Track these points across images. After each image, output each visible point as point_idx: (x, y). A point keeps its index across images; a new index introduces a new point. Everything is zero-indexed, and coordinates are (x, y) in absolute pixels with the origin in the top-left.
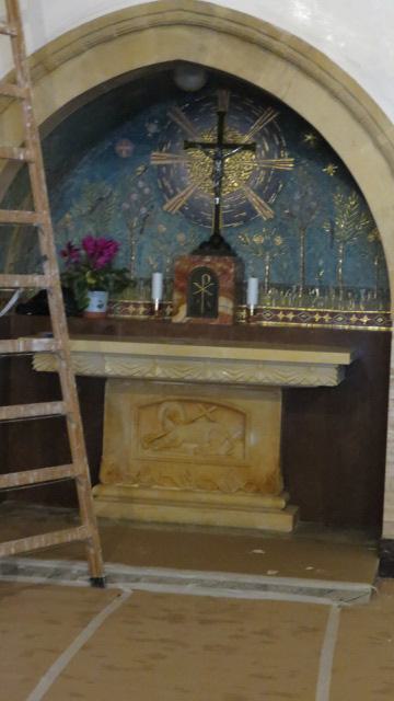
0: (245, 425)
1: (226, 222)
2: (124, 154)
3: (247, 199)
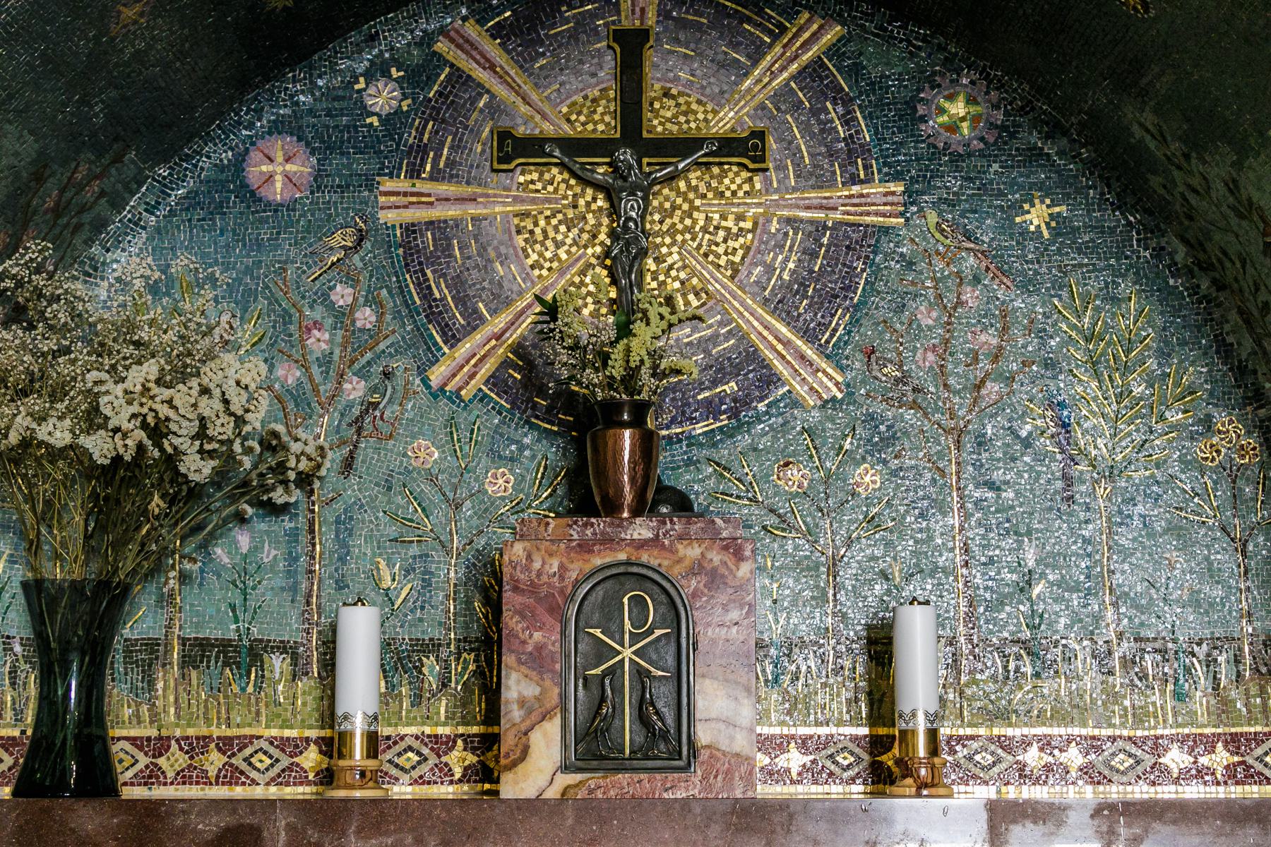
2: (278, 191)
3: (735, 333)
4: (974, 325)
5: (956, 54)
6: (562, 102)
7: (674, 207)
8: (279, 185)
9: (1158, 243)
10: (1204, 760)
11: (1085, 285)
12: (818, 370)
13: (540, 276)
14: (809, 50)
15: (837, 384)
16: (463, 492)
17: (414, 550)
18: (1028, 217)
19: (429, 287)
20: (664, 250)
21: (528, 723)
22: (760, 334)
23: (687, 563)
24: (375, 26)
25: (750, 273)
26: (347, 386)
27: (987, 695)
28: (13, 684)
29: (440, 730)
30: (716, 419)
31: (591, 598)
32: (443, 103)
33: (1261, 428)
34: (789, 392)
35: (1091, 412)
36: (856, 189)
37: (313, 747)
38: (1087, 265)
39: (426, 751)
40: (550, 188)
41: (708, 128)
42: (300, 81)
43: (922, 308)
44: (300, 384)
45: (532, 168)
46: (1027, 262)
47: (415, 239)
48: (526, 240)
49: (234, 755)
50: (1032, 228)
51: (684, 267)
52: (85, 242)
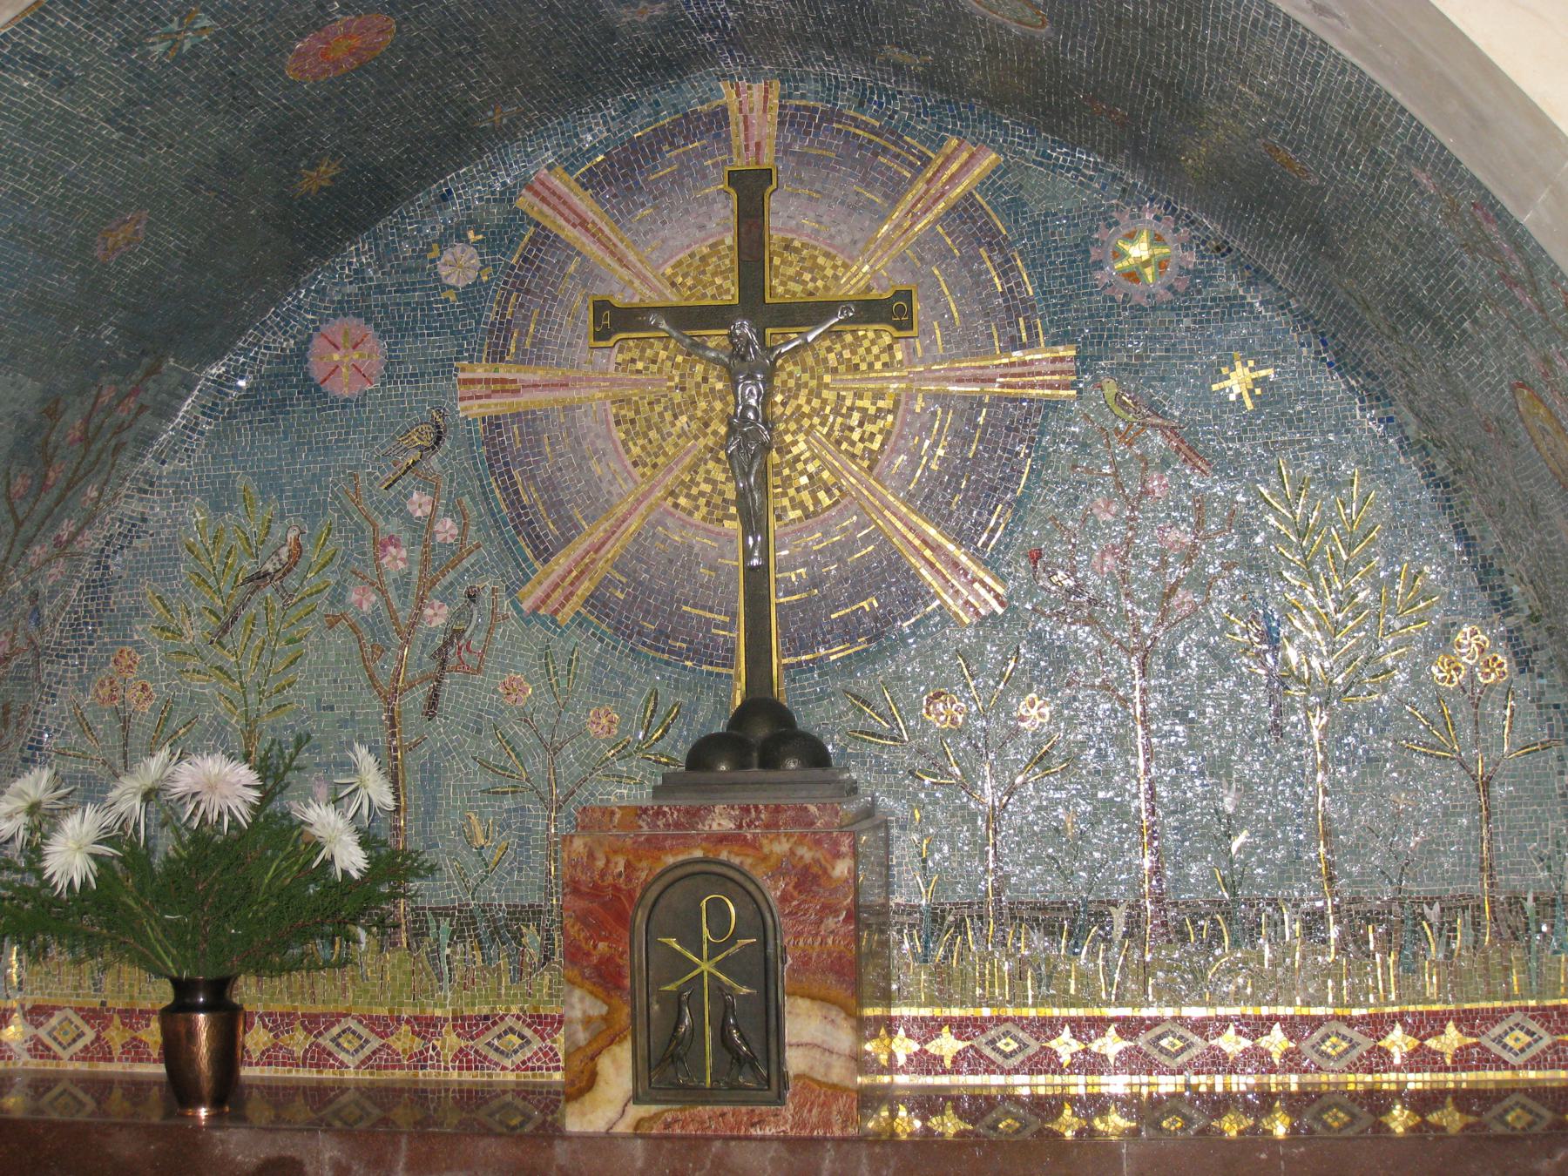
1: (796, 644)
2: (343, 386)
4: (1160, 520)
5: (1135, 185)
6: (665, 262)
7: (799, 387)
9: (1386, 413)
11: (1299, 466)
12: (973, 581)
13: (643, 475)
14: (956, 185)
15: (997, 596)
17: (508, 803)
18: (1227, 383)
19: (517, 492)
21: (595, 1046)
22: (905, 537)
23: (773, 860)
24: (446, 184)
25: (891, 463)
26: (428, 612)
30: (853, 642)
31: (662, 902)
32: (528, 270)
33: (1510, 639)
34: (940, 607)
35: (1306, 624)
37: (405, 1028)
38: (1299, 442)
39: (528, 1033)
40: (654, 368)
41: (839, 287)
42: (365, 253)
43: (1100, 501)
44: (376, 612)
45: (631, 343)
46: (1227, 440)
47: (500, 435)
48: (627, 432)
49: (320, 1034)
50: (1232, 397)
51: (813, 458)
52: (133, 459)
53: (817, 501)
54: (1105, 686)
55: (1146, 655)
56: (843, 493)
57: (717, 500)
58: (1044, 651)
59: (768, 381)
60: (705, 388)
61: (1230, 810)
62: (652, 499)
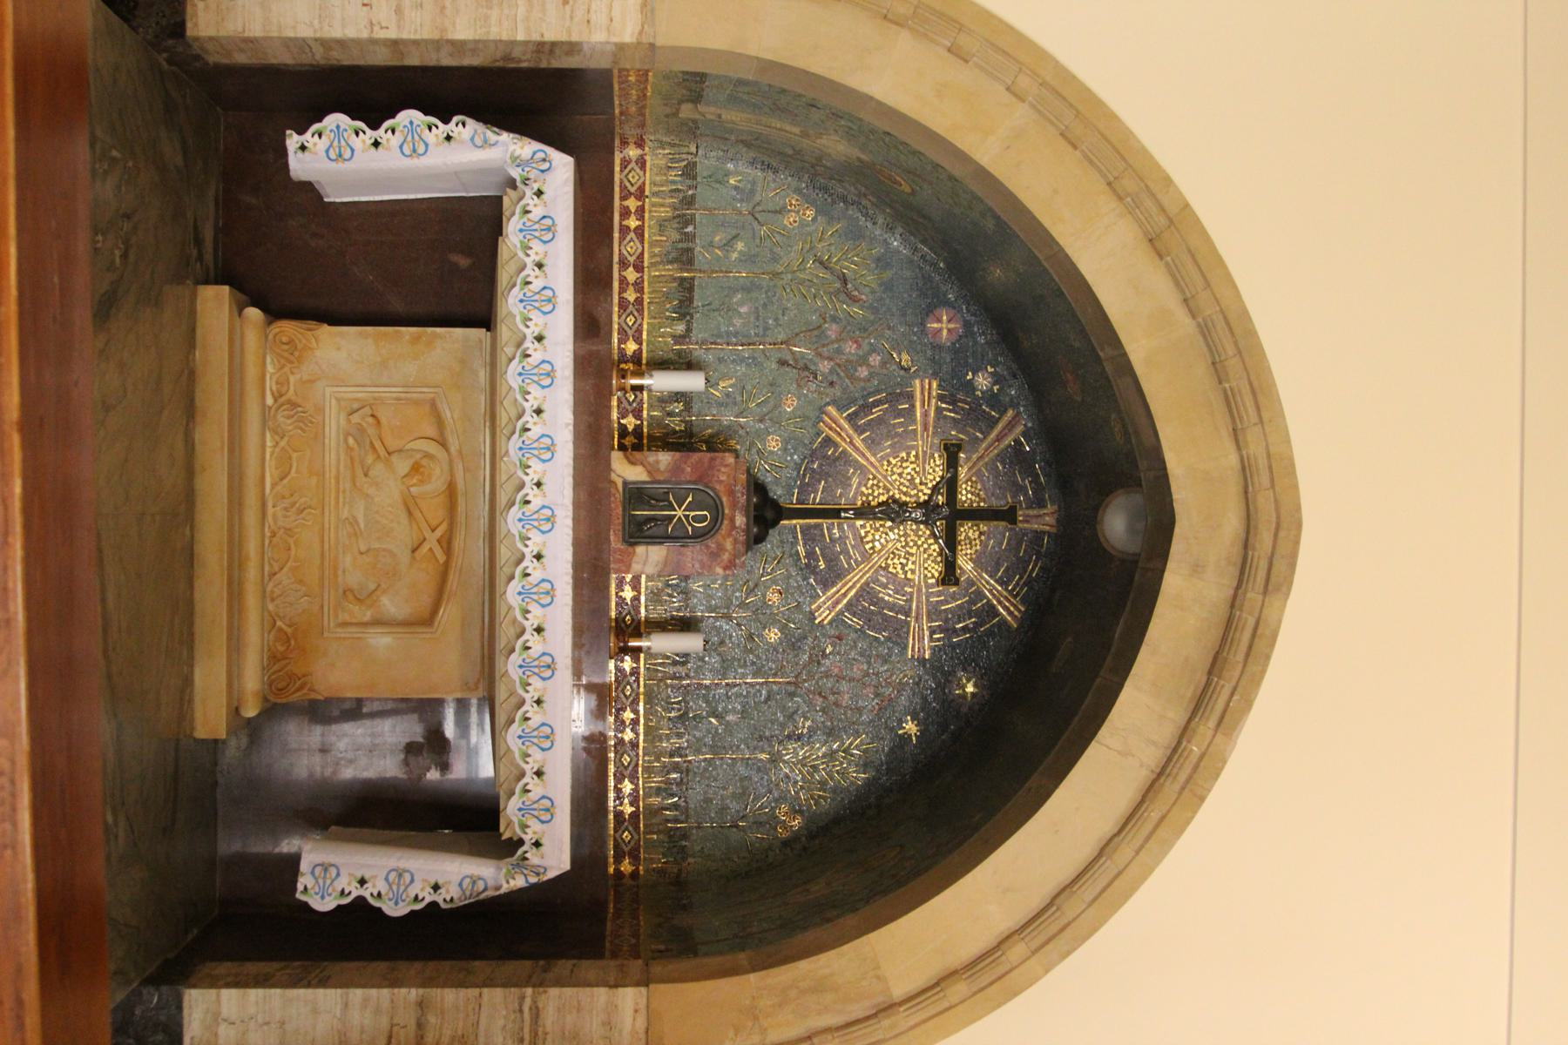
0: (405, 623)
1: (806, 530)
8: (935, 325)
10: (626, 801)
16: (768, 423)
20: (896, 531)
21: (646, 464)
27: (659, 693)
28: (671, 191)
29: (645, 412)
36: (927, 633)
39: (634, 405)
40: (931, 471)
44: (827, 337)
51: (887, 542)
53: (868, 543)
54: (783, 667)
55: (796, 684)
56: (871, 555)
57: (871, 498)
58: (799, 640)
59: (922, 522)
60: (920, 494)
61: (727, 718)
62: (872, 470)
